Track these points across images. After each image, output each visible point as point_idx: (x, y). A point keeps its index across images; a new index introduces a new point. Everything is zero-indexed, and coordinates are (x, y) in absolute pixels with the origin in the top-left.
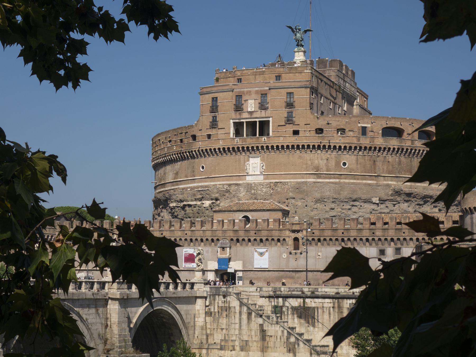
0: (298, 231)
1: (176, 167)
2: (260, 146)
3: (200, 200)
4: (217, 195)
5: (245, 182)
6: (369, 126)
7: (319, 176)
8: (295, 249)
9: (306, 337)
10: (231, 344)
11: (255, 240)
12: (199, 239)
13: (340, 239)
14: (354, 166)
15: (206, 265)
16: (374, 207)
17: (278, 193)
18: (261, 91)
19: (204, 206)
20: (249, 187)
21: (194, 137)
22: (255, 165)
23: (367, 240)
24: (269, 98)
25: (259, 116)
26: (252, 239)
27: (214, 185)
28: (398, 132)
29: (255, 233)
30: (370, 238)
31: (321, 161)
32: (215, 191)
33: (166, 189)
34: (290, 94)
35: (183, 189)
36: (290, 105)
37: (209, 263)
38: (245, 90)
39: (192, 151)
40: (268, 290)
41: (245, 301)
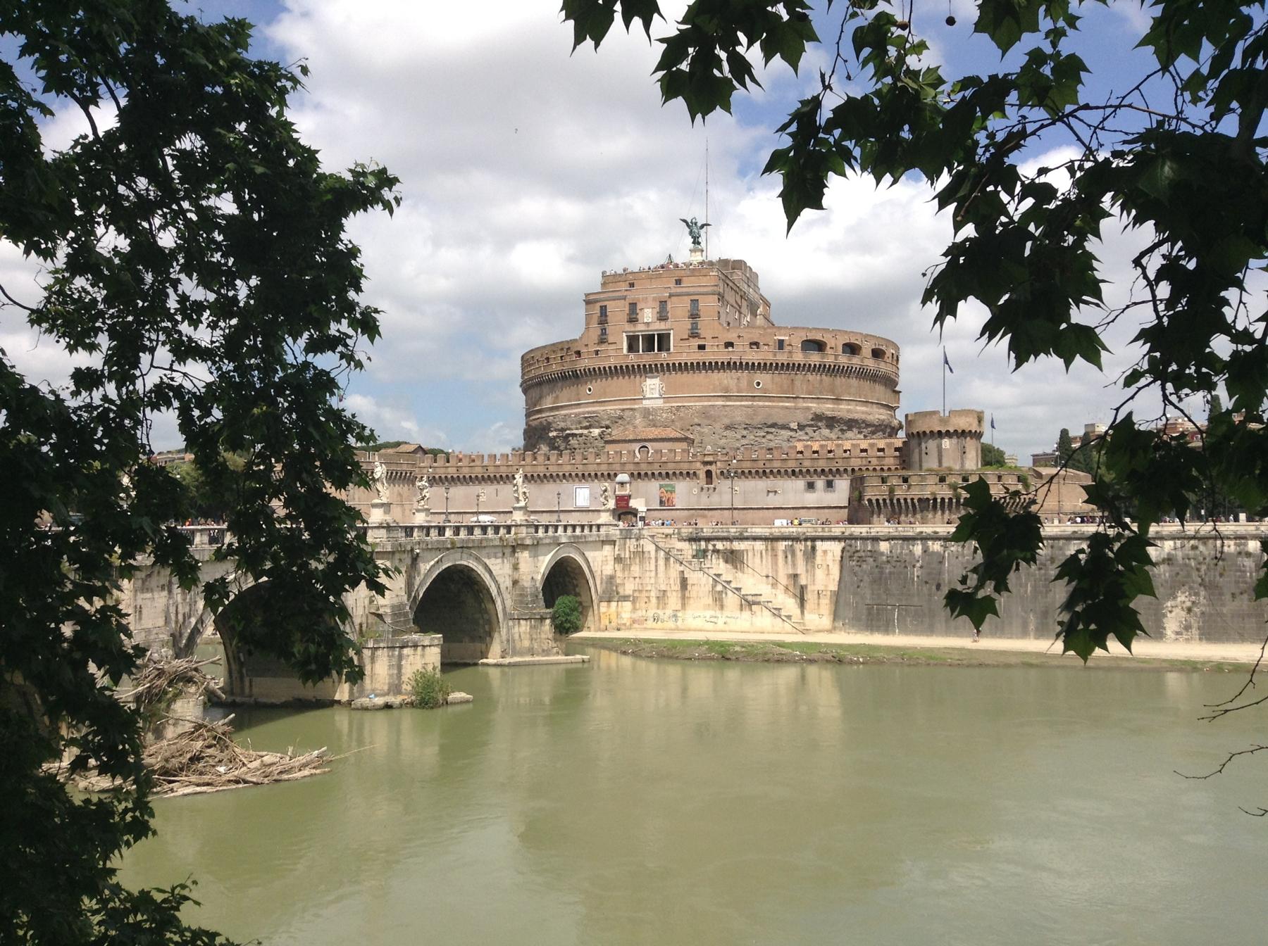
0: (710, 463)
3: (586, 428)
9: (733, 585)
10: (644, 594)
14: (769, 386)
16: (792, 434)
17: (681, 419)
20: (647, 412)
21: (578, 353)
22: (653, 386)
23: (793, 471)
24: (669, 306)
28: (819, 346)
34: (695, 302)
36: (694, 316)
40: (686, 531)
41: (661, 545)
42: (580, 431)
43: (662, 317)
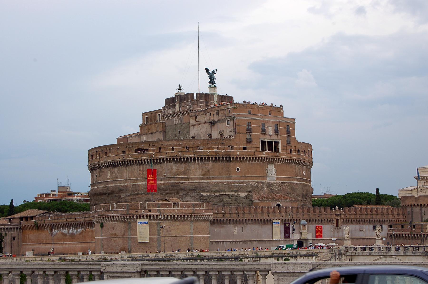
1: (207, 166)
2: (275, 158)
3: (235, 191)
4: (251, 189)
7: (298, 180)
13: (358, 220)
19: (240, 196)
20: (269, 185)
24: (279, 127)
25: (274, 138)
26: (317, 220)
30: (371, 220)
32: (250, 186)
33: (191, 181)
35: (217, 183)
36: (288, 133)
39: (230, 157)
42: (233, 193)
43: (276, 132)
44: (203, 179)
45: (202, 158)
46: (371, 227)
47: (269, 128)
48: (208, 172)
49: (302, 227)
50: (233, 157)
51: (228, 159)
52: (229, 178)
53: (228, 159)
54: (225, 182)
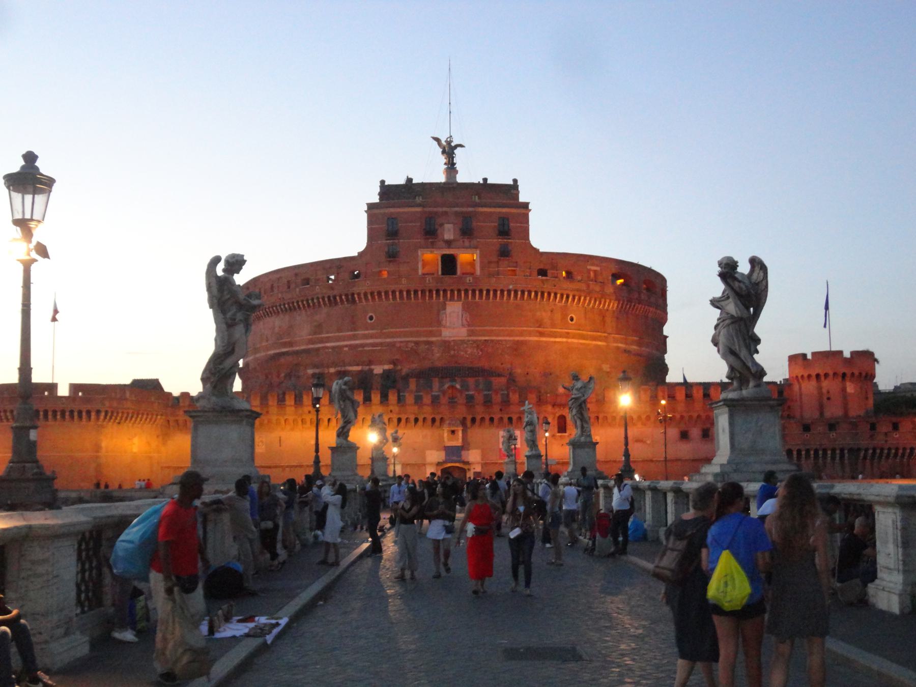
2: (462, 288)
4: (397, 357)
5: (439, 338)
6: (598, 268)
7: (541, 334)
8: (559, 432)
11: (501, 419)
12: (412, 418)
15: (424, 458)
18: (462, 213)
19: (375, 372)
27: (390, 343)
29: (501, 410)
31: (544, 314)
33: (297, 348)
35: (333, 348)
37: (428, 453)
38: (440, 210)
39: (353, 294)
44: (311, 342)
45: (307, 301)
46: (673, 432)
47: (447, 226)
48: (318, 328)
49: (446, 435)
50: (359, 294)
51: (351, 299)
52: (354, 337)
53: (351, 299)
54: (346, 346)
